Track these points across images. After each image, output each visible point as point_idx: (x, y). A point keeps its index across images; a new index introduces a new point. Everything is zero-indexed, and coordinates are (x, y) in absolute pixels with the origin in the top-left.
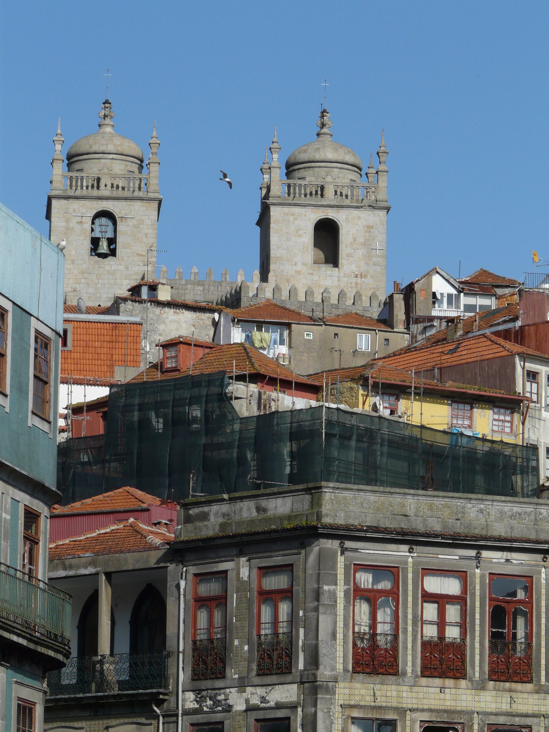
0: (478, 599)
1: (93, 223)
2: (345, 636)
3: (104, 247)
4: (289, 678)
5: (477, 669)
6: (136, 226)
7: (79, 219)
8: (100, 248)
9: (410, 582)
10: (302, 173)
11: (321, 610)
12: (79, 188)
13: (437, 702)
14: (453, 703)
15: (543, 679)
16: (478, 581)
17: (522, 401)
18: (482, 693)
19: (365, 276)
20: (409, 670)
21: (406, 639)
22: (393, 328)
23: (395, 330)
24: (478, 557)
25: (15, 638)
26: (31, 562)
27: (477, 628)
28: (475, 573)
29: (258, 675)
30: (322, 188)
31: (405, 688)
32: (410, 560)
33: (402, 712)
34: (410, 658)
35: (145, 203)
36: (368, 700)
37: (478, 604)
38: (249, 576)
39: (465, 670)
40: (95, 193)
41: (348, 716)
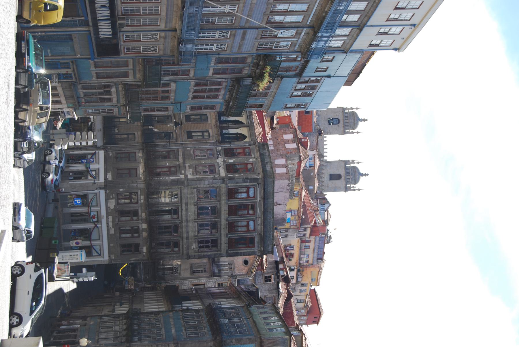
0: (248, 218)
1: (337, 119)
2: (237, 186)
4: (226, 173)
5: (231, 219)
9: (251, 201)
15: (230, 235)
16: (253, 218)
20: (230, 202)
27: (241, 218)
30: (349, 175)
34: (233, 202)
36: (222, 192)
37: (247, 218)
41: (217, 188)
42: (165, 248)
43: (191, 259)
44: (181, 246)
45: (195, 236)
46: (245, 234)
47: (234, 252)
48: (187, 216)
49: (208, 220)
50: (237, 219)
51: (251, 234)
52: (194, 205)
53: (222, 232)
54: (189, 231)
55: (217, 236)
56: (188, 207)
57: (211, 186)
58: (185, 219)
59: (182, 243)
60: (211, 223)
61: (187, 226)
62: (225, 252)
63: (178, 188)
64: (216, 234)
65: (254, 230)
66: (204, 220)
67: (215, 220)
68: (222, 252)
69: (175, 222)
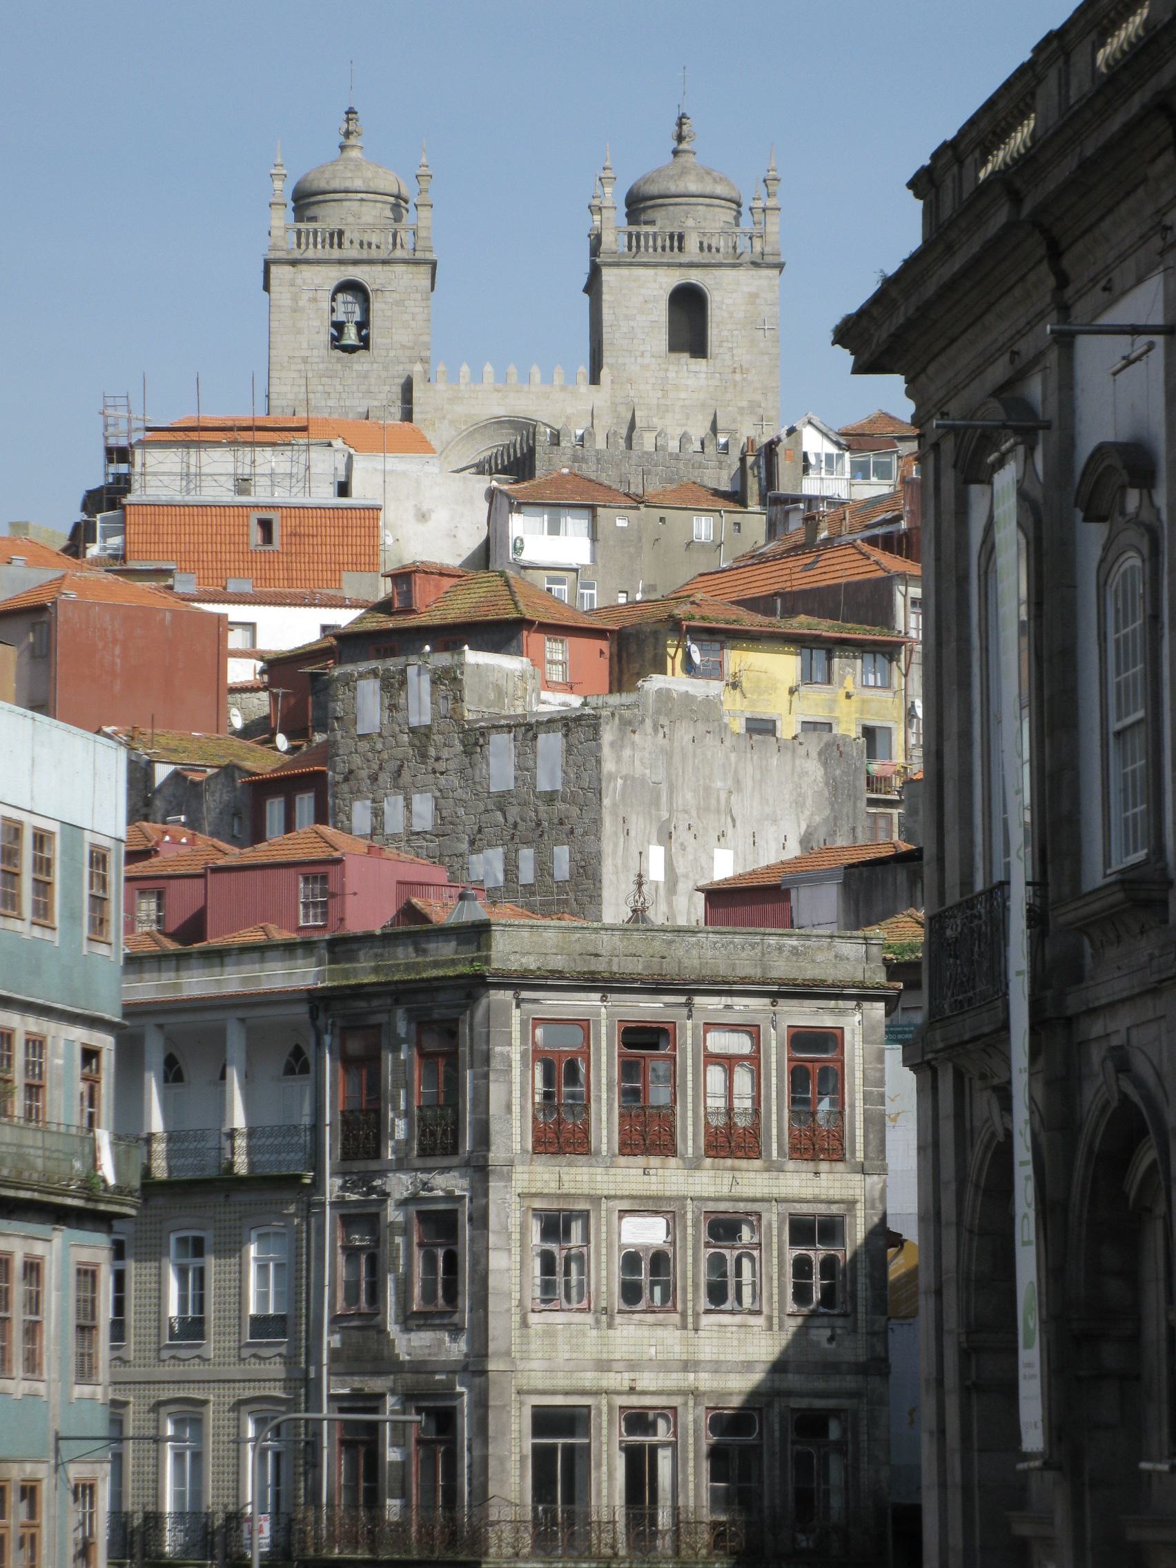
0: (689, 1055)
1: (333, 300)
2: (522, 1108)
3: (351, 337)
4: (454, 1161)
5: (690, 1143)
6: (400, 303)
7: (311, 294)
8: (346, 336)
9: (604, 1037)
10: (650, 215)
11: (492, 1076)
12: (311, 246)
13: (640, 1187)
14: (661, 1187)
16: (689, 1033)
17: (903, 643)
18: (698, 1173)
19: (748, 370)
20: (604, 1147)
21: (600, 1110)
22: (746, 507)
23: (750, 509)
24: (689, 1005)
25: (69, 1201)
26: (91, 1105)
27: (690, 1092)
28: (685, 1025)
29: (419, 1156)
30: (681, 237)
31: (599, 1170)
32: (603, 1010)
33: (596, 1199)
34: (604, 1132)
35: (411, 268)
36: (552, 1188)
37: (690, 1062)
38: (407, 1033)
39: (675, 1145)
40: (336, 253)
41: (528, 1208)
42: (827, 1482)
43: (887, 1351)
44: (819, 1403)
45: (770, 1328)
46: (774, 1073)
47: (859, 1132)
48: (664, 1366)
49: (690, 1260)
50: (690, 1114)
51: (774, 1043)
52: (610, 1326)
53: (758, 1192)
54: (742, 1358)
55: (775, 1218)
56: (617, 1356)
57: (516, 1236)
58: (681, 1375)
59: (801, 1395)
60: (708, 1245)
61: (717, 1367)
62: (859, 1177)
63: (522, 1403)
64: (764, 1222)
65: (753, 1031)
66: (690, 1282)
67: (689, 1223)
68: (858, 1193)
69: (691, 1426)
